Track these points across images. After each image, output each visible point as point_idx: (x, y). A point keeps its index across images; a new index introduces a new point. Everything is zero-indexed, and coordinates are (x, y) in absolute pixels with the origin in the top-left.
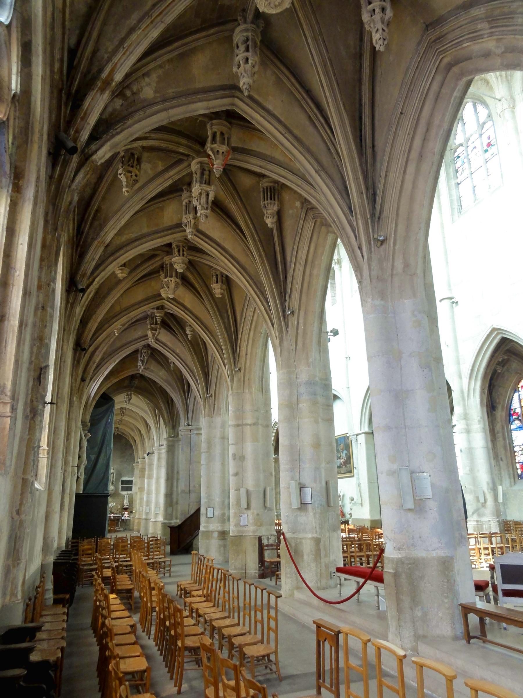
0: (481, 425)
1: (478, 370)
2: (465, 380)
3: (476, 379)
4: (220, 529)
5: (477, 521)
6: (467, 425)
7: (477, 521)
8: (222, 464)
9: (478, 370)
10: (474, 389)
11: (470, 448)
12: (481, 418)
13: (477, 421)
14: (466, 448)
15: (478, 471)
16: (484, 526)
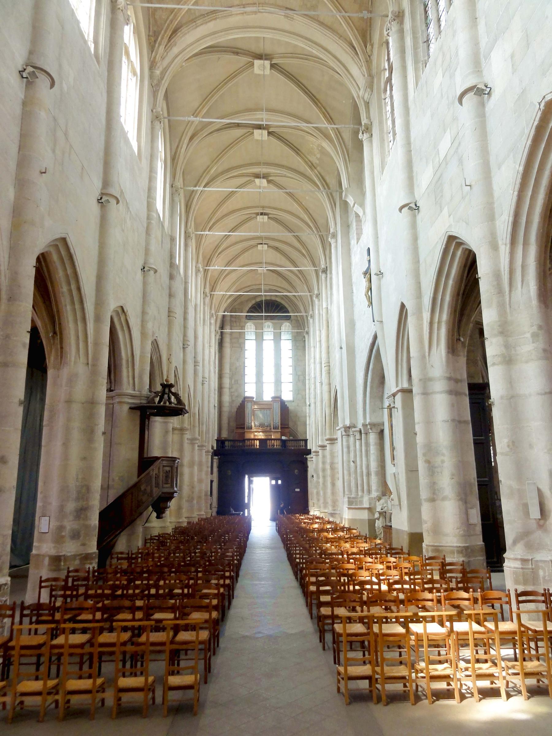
0: (541, 344)
1: (528, 223)
2: (504, 250)
3: (526, 243)
4: (53, 552)
5: (524, 561)
6: (507, 346)
7: (524, 561)
8: (64, 444)
9: (528, 223)
10: (523, 267)
11: (512, 397)
12: (540, 327)
13: (528, 335)
14: (502, 398)
15: (531, 446)
16: (541, 573)
